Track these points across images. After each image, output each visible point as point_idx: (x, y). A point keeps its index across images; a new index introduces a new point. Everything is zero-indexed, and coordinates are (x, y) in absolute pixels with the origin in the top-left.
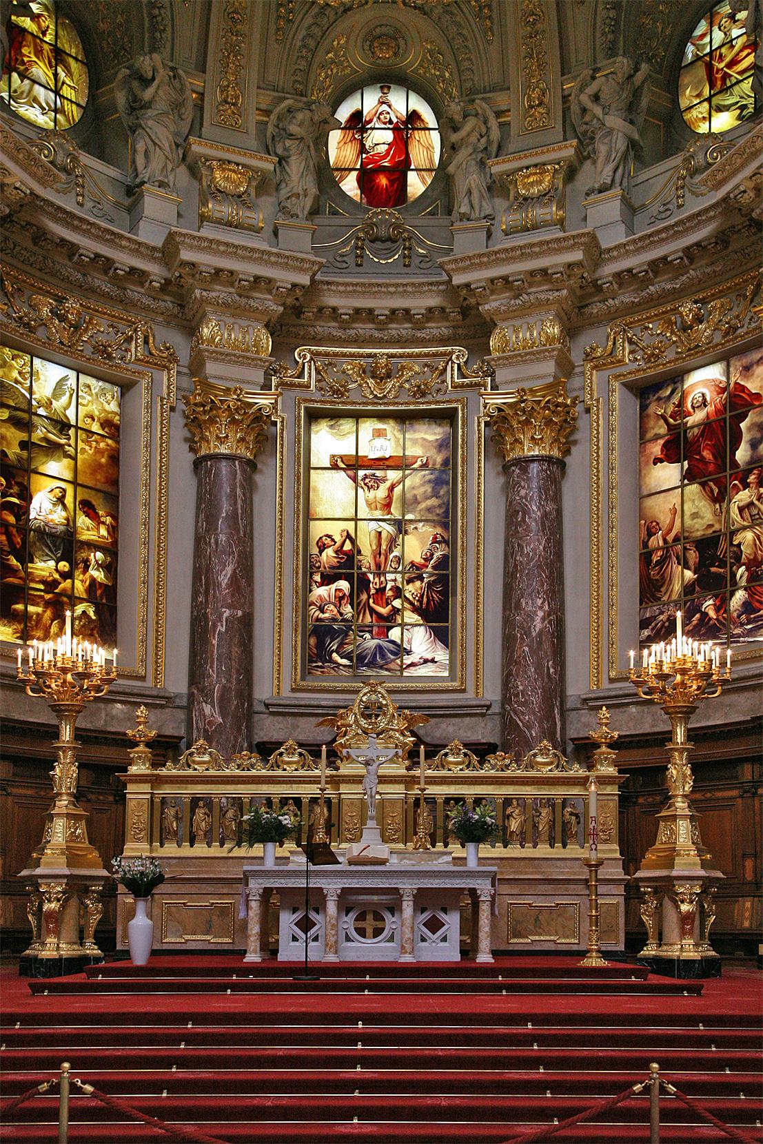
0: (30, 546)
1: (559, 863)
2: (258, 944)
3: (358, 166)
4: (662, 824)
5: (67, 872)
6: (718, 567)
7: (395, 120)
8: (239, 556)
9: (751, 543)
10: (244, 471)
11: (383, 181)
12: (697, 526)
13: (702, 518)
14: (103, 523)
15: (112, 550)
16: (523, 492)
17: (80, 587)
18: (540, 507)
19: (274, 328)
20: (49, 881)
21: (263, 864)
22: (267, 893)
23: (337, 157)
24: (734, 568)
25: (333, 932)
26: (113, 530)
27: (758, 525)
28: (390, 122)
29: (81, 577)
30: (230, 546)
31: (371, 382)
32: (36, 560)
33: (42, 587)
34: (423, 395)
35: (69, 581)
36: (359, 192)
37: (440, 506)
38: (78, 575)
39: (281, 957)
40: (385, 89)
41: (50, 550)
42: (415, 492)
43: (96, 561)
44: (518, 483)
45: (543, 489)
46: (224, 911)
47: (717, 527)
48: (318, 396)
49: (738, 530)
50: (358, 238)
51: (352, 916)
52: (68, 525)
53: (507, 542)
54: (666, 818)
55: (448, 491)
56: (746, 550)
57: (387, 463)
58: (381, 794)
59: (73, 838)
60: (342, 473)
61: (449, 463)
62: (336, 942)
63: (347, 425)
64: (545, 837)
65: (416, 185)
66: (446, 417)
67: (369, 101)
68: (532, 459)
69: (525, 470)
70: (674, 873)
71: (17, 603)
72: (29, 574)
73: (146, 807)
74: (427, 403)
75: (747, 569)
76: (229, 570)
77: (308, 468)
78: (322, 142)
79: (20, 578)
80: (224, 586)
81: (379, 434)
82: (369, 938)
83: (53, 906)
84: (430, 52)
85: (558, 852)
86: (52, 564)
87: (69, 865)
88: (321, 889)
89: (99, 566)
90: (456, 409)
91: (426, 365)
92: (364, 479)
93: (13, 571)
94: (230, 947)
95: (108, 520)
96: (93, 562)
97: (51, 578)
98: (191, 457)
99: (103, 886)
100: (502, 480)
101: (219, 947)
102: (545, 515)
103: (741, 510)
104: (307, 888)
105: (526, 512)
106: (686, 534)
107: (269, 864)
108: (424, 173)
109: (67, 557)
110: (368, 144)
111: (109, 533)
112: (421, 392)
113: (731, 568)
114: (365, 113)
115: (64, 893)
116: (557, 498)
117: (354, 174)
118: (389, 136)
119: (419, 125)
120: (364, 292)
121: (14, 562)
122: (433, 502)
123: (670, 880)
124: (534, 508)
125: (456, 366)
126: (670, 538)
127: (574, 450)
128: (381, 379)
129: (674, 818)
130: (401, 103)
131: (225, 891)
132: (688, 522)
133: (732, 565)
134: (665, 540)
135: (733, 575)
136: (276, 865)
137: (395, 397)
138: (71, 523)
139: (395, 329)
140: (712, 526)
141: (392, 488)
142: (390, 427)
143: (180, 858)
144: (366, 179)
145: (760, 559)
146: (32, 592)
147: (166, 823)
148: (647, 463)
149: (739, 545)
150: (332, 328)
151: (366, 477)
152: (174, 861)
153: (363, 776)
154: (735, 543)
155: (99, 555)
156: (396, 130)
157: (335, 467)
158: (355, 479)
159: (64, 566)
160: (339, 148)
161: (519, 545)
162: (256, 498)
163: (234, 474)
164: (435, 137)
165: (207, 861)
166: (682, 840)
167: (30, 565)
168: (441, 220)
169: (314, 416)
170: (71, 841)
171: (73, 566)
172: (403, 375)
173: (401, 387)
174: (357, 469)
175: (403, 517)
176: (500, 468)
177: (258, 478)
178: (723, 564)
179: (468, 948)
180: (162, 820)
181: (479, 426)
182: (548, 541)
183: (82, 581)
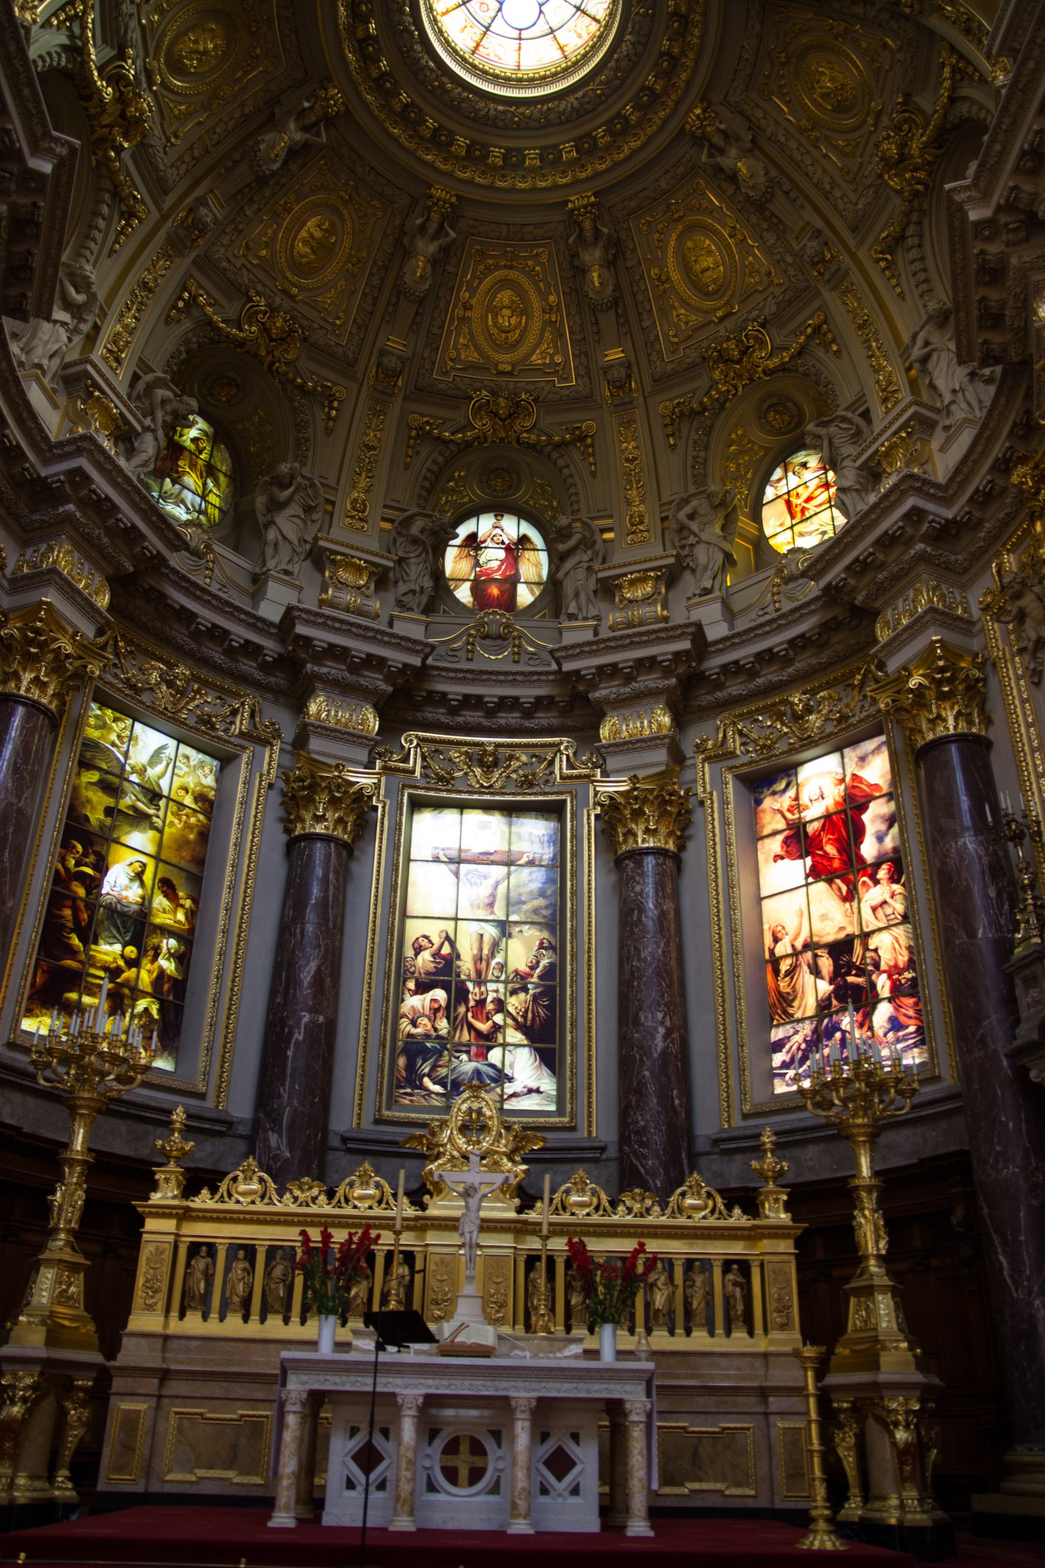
0: (97, 926)
1: (723, 1361)
2: (293, 1494)
3: (472, 577)
4: (853, 1301)
5: (43, 1353)
6: (856, 975)
7: (507, 542)
8: (326, 950)
9: (890, 946)
10: (339, 855)
11: (495, 591)
12: (828, 930)
13: (833, 920)
14: (182, 906)
15: (187, 938)
16: (638, 888)
17: (145, 978)
18: (658, 905)
19: (381, 712)
20: (16, 1367)
21: (316, 1351)
22: (316, 1399)
23: (453, 570)
24: (874, 977)
25: (408, 1474)
26: (191, 915)
27: (895, 925)
28: (503, 543)
29: (149, 966)
30: (317, 938)
31: (478, 771)
32: (101, 941)
33: (102, 974)
34: (531, 785)
35: (134, 970)
36: (471, 599)
37: (546, 907)
38: (146, 964)
39: (331, 1517)
40: (499, 516)
41: (119, 932)
42: (521, 890)
43: (169, 949)
44: (633, 878)
45: (660, 886)
46: (256, 1427)
47: (850, 930)
48: (423, 784)
49: (873, 932)
50: (470, 635)
51: (439, 1443)
52: (142, 904)
53: (622, 945)
54: (860, 1292)
55: (555, 892)
56: (886, 958)
57: (492, 858)
58: (481, 1247)
59: (62, 1298)
60: (443, 866)
61: (559, 863)
62: (412, 1493)
63: (450, 816)
64: (700, 1318)
65: (525, 596)
66: (552, 810)
67: (484, 525)
68: (648, 852)
69: (639, 864)
70: (882, 1378)
71: (71, 991)
72: (93, 957)
73: (167, 1256)
74: (535, 794)
75: (890, 977)
76: (313, 966)
77: (408, 860)
78: (439, 553)
79: (80, 962)
80: (306, 983)
81: (484, 826)
82: (463, 1486)
83: (16, 1410)
84: (541, 486)
85: (720, 1343)
86: (117, 948)
87: (52, 1340)
88: (393, 1395)
89: (171, 955)
90: (564, 801)
91: (534, 756)
92: (466, 875)
93: (72, 953)
94: (260, 1493)
95: (188, 903)
96: (164, 950)
97: (114, 965)
98: (284, 838)
99: (94, 1380)
100: (613, 878)
101: (244, 1492)
102: (663, 915)
103: (874, 909)
104: (374, 1393)
105: (641, 910)
106: (815, 939)
107: (326, 1350)
108: (534, 587)
109: (137, 941)
110: (482, 560)
111: (187, 918)
112: (528, 783)
113: (870, 976)
114: (480, 535)
115: (34, 1387)
116: (676, 896)
117: (468, 585)
118: (502, 554)
119: (528, 546)
120: (474, 680)
121: (75, 941)
122: (540, 902)
123: (876, 1387)
124: (651, 905)
125: (564, 758)
126: (799, 945)
127: (691, 846)
128: (488, 768)
129: (869, 1291)
130: (511, 528)
131: (261, 1395)
132: (817, 926)
133: (872, 972)
134: (793, 946)
135: (873, 985)
136: (334, 1351)
137: (503, 787)
138: (146, 902)
139: (505, 718)
140: (842, 929)
141: (496, 887)
142: (496, 821)
143: (203, 1339)
144: (478, 588)
145: (901, 965)
146: (90, 979)
147: (190, 1283)
148: (767, 860)
149: (876, 950)
150: (439, 714)
151: (469, 872)
152: (194, 1344)
153: (457, 1219)
154: (871, 947)
155: (173, 943)
156: (508, 549)
157: (436, 860)
158: (457, 874)
159: (131, 951)
160: (455, 562)
161: (636, 948)
162: (351, 889)
163: (328, 856)
164: (543, 557)
165: (240, 1345)
166: (884, 1325)
167: (93, 947)
168: (553, 624)
169: (417, 805)
170: (60, 1303)
171: (142, 952)
172: (509, 766)
173: (508, 777)
174: (459, 863)
175: (508, 916)
176: (612, 865)
177: (355, 867)
178: (861, 972)
179: (607, 1503)
180: (186, 1276)
181: (589, 818)
182: (667, 944)
183: (149, 971)
